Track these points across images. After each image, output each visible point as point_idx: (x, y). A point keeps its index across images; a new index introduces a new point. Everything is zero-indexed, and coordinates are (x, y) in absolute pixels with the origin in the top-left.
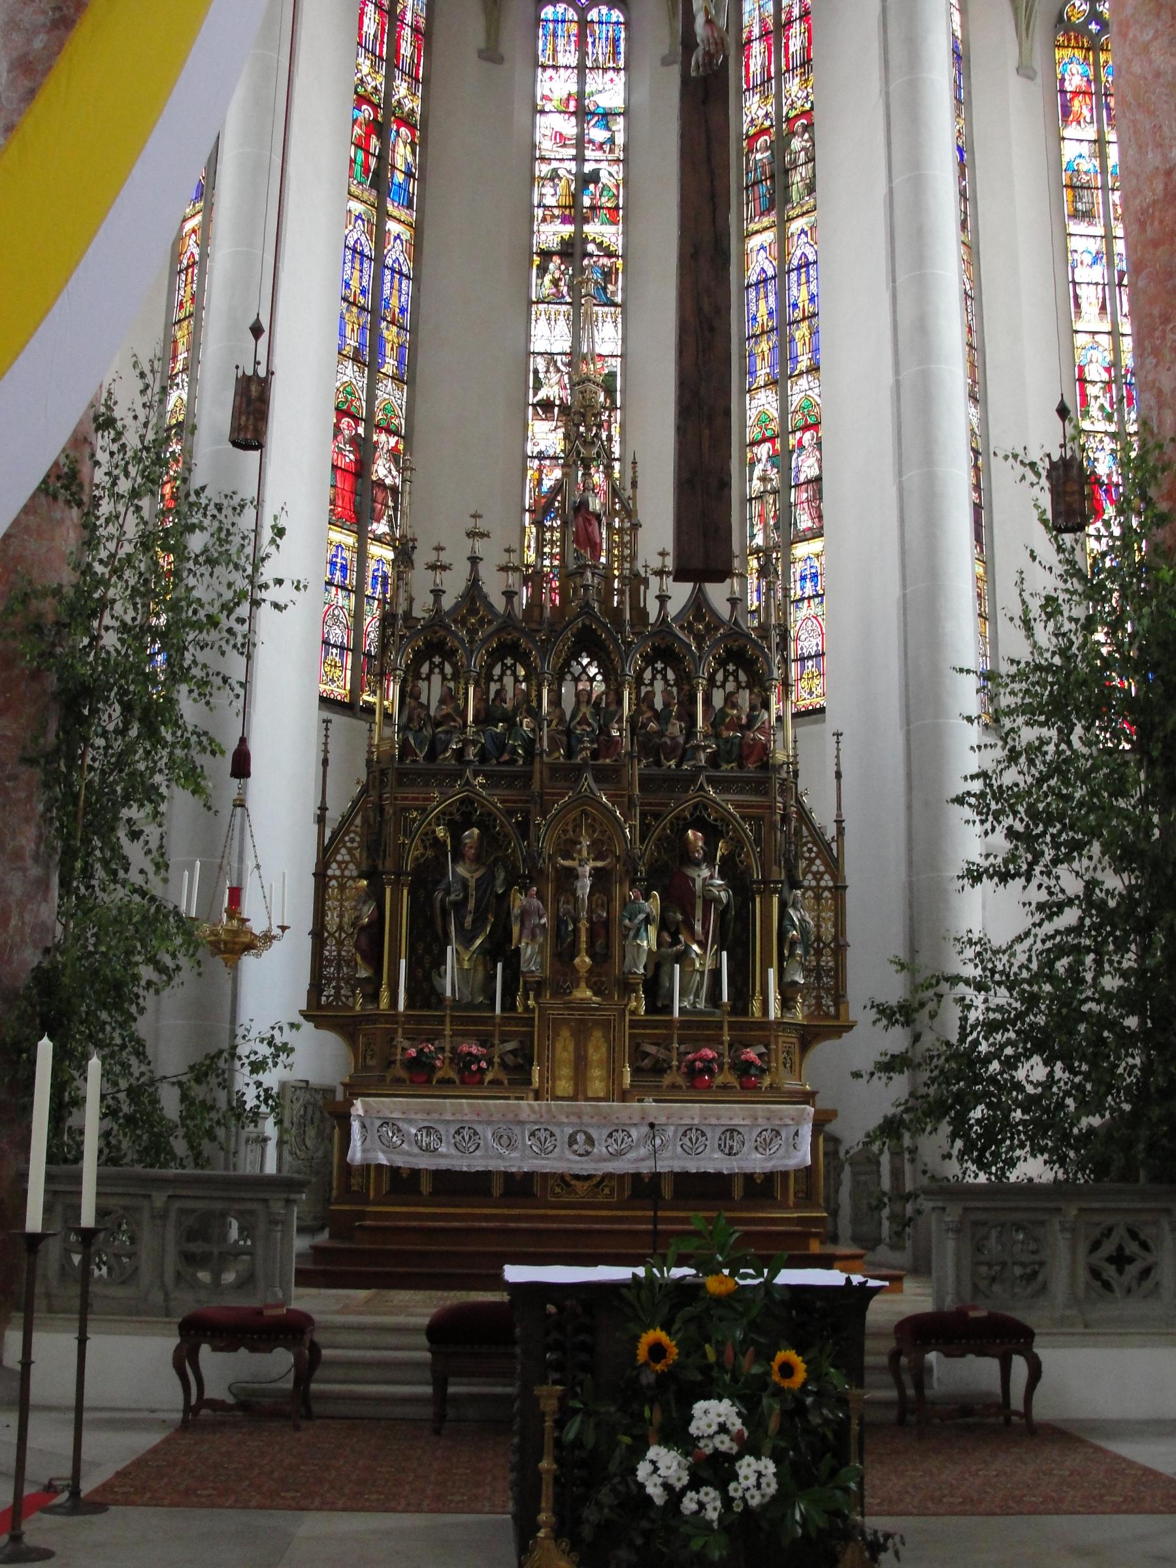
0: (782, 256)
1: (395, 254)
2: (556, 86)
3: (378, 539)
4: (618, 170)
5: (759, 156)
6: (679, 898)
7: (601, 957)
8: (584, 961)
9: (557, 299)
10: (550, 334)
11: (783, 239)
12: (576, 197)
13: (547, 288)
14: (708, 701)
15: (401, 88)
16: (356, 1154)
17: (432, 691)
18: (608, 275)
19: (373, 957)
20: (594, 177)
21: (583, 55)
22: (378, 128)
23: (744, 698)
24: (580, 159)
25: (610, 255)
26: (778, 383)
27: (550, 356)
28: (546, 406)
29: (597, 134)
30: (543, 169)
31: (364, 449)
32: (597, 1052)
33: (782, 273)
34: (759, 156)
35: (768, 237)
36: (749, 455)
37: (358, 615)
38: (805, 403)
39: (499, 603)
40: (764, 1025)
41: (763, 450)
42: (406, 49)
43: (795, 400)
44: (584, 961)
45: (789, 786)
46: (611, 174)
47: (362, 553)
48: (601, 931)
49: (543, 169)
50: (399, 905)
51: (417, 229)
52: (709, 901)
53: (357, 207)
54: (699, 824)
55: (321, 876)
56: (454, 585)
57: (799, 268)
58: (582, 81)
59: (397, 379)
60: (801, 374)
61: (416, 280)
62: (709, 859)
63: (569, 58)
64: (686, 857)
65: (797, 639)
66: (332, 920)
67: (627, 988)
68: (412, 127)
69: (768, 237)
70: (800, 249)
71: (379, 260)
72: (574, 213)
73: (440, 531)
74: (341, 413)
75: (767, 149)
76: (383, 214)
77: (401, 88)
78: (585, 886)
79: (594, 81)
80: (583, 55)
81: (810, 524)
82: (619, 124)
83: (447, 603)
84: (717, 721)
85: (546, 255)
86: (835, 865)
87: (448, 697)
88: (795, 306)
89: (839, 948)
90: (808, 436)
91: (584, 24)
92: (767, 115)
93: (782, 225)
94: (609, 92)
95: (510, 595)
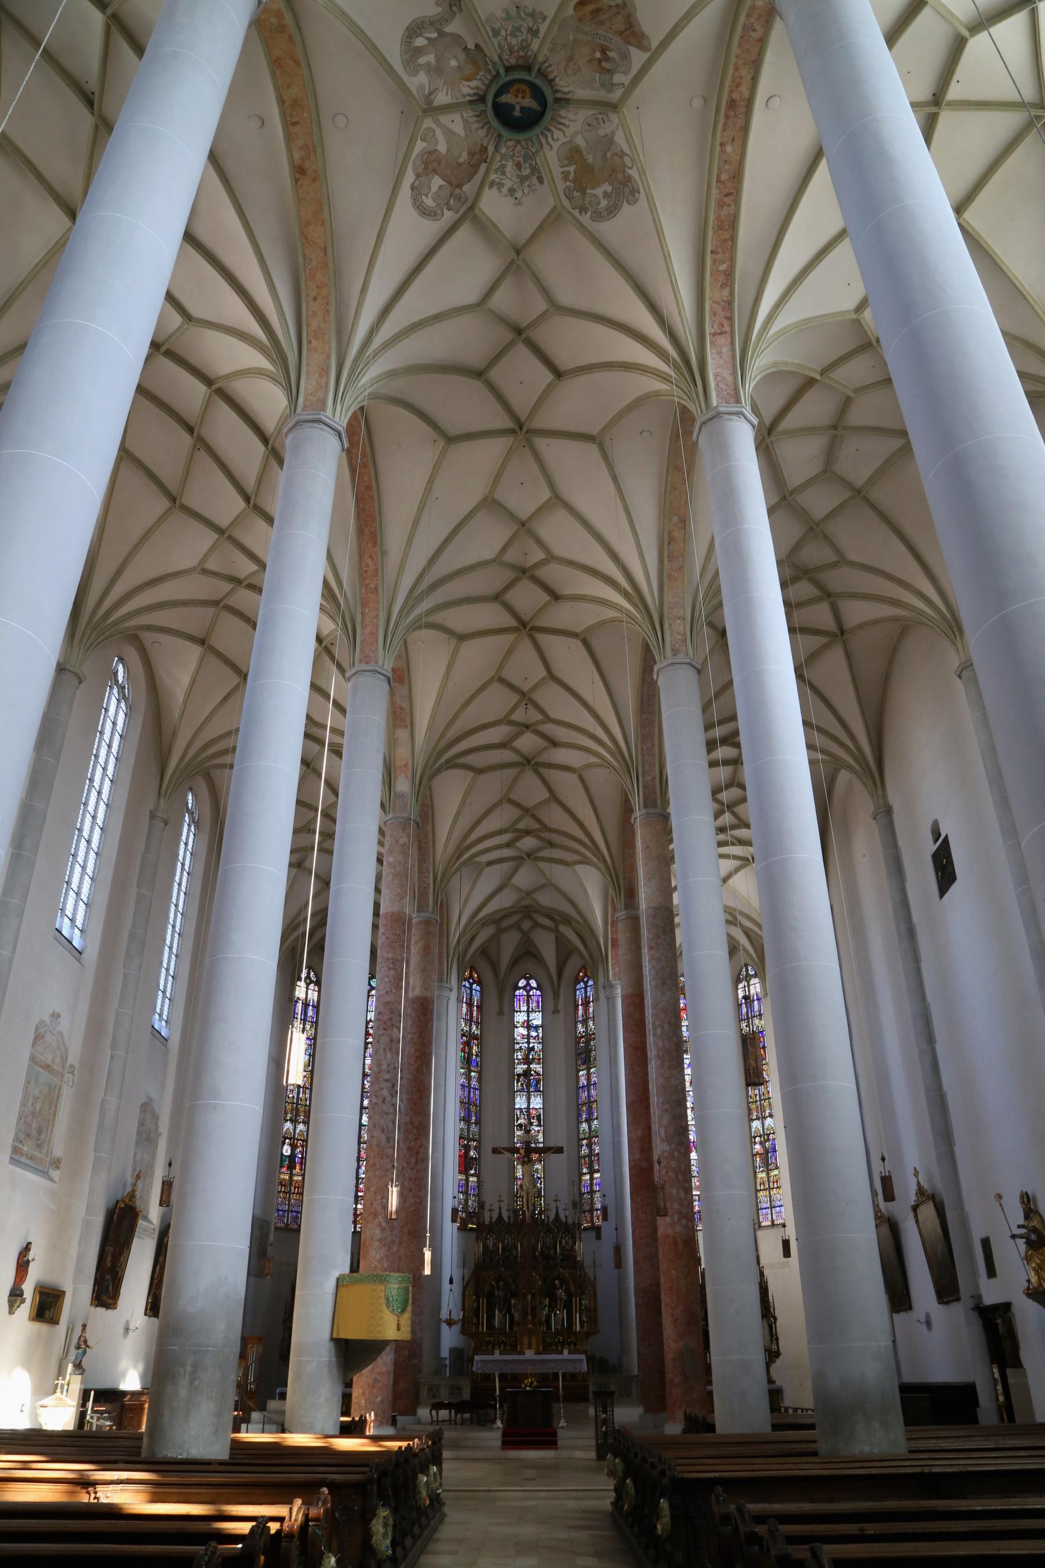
0: (589, 1079)
1: (474, 1083)
2: (520, 1018)
3: (472, 1175)
4: (540, 1046)
6: (554, 1299)
7: (534, 1316)
8: (530, 1317)
9: (522, 1090)
10: (520, 1102)
11: (589, 1074)
12: (527, 1055)
13: (520, 1087)
14: (561, 1243)
15: (474, 1028)
16: (474, 1369)
17: (490, 1243)
18: (538, 1082)
19: (478, 1317)
20: (533, 1048)
21: (528, 1007)
22: (467, 1044)
23: (570, 1242)
24: (528, 1043)
25: (538, 1075)
26: (589, 1121)
27: (521, 1109)
28: (520, 1125)
29: (534, 1034)
30: (517, 1047)
31: (467, 1148)
32: (534, 1341)
33: (589, 1085)
35: (585, 1072)
37: (466, 1200)
39: (506, 1220)
40: (576, 1332)
41: (584, 1142)
42: (475, 1014)
44: (530, 1317)
45: (582, 1267)
46: (538, 1047)
47: (467, 1180)
48: (534, 1309)
49: (517, 1047)
50: (483, 1302)
51: (480, 1073)
52: (561, 1299)
53: (462, 1071)
54: (558, 1279)
55: (464, 1295)
56: (495, 1215)
58: (528, 1016)
59: (476, 1123)
61: (480, 1090)
62: (561, 1287)
63: (524, 1008)
64: (555, 1287)
66: (467, 1305)
67: (541, 1324)
68: (477, 1039)
69: (585, 1072)
70: (594, 1079)
71: (469, 1086)
72: (527, 1061)
73: (490, 1199)
74: (460, 1138)
76: (470, 1071)
77: (474, 1028)
78: (530, 1296)
79: (532, 1016)
80: (528, 1007)
82: (540, 1030)
83: (494, 1220)
84: (562, 1249)
85: (519, 1075)
86: (594, 1287)
87: (495, 1245)
89: (596, 1309)
91: (529, 996)
93: (588, 1069)
94: (537, 1019)
95: (509, 1218)
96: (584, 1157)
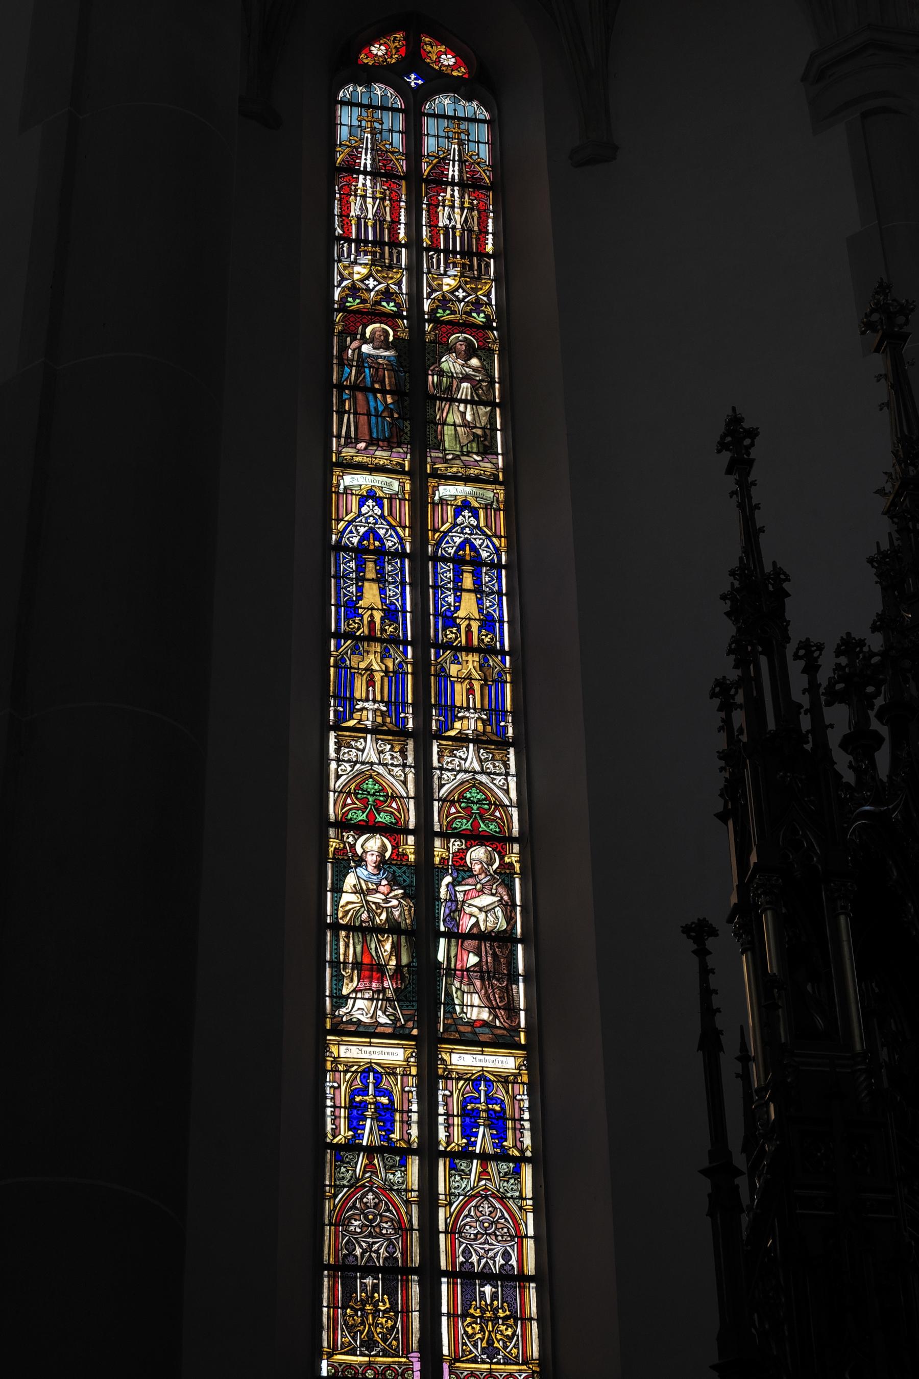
5: (366, 349)
34: (366, 349)
36: (334, 844)
38: (473, 794)
43: (447, 784)
57: (458, 562)
60: (462, 740)
65: (453, 1231)
75: (386, 345)
81: (485, 1015)
88: (450, 621)
90: (478, 853)
92: (387, 295)
96: (364, 931)
